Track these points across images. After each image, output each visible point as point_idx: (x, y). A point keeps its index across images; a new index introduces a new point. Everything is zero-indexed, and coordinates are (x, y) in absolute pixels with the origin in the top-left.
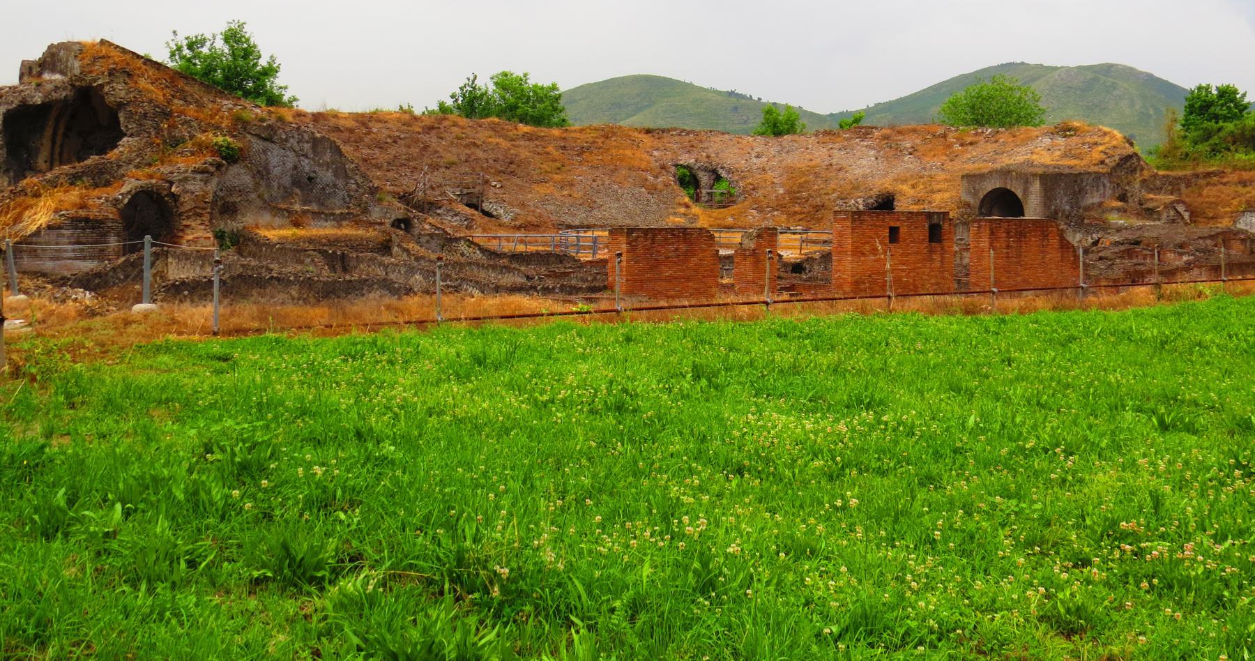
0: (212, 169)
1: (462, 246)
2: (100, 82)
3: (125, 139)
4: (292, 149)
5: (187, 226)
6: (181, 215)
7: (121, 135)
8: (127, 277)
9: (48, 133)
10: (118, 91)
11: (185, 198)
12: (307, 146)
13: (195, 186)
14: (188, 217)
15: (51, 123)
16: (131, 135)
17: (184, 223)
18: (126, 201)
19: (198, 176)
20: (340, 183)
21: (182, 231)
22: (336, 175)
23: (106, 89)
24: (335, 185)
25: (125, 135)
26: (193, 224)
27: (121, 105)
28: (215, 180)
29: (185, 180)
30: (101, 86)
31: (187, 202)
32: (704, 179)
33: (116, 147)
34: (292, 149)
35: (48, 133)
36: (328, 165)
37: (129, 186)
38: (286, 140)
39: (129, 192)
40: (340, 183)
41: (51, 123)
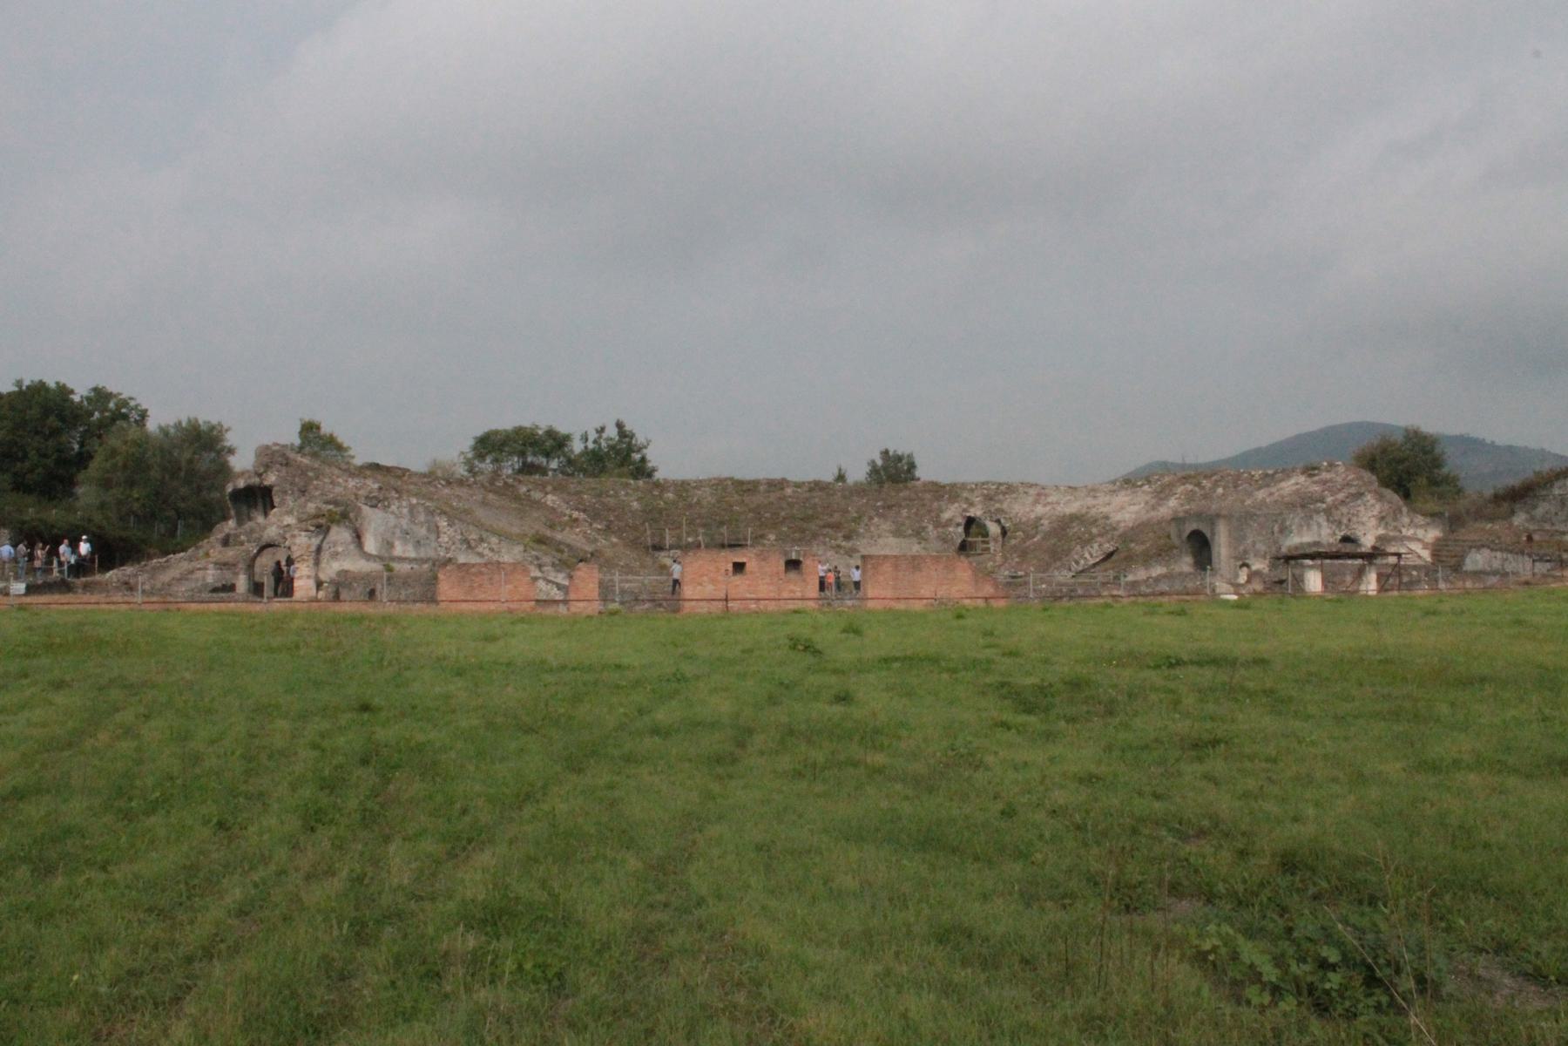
7: (273, 507)
11: (294, 548)
12: (405, 511)
22: (428, 530)
36: (422, 524)
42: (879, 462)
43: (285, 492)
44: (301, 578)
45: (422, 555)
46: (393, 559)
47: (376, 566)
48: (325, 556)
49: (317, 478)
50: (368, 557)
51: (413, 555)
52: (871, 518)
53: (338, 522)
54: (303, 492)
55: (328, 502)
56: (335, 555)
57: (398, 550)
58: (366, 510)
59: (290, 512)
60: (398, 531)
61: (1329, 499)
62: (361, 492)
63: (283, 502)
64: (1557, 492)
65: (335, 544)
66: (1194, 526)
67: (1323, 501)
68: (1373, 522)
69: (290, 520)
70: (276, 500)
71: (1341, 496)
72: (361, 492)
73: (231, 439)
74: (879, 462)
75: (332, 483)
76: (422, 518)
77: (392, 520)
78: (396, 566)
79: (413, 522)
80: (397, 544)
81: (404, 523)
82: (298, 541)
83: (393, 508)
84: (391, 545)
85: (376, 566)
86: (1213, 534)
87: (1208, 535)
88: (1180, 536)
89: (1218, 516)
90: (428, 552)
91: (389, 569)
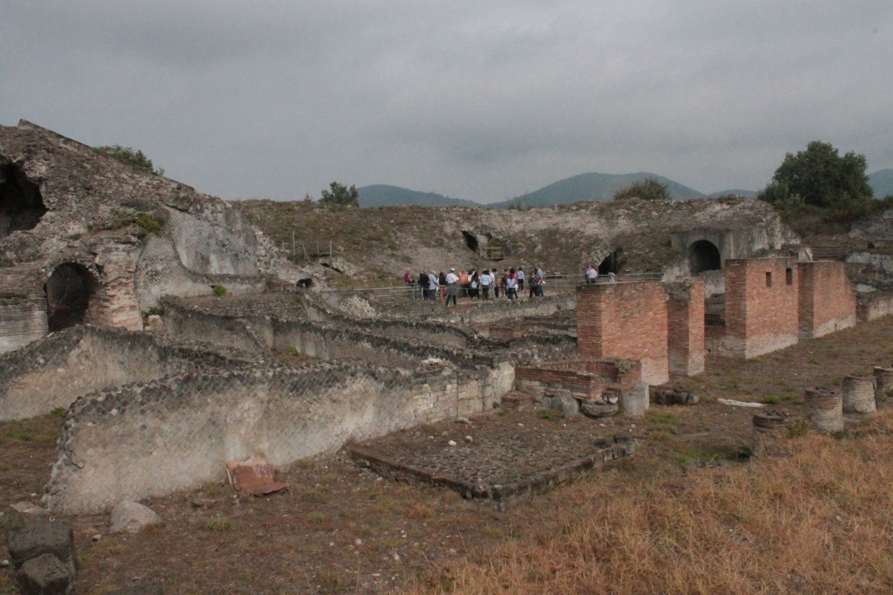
0: (134, 239)
2: (19, 158)
3: (48, 214)
4: (206, 219)
5: (113, 296)
6: (106, 285)
8: (47, 361)
10: (39, 169)
11: (109, 268)
12: (220, 216)
14: (113, 287)
16: (54, 209)
17: (111, 293)
18: (50, 274)
19: (121, 246)
21: (108, 301)
22: (247, 242)
23: (26, 165)
24: (246, 251)
25: (48, 210)
26: (118, 294)
27: (41, 180)
30: (21, 162)
31: (112, 272)
33: (39, 221)
34: (206, 219)
38: (202, 211)
39: (52, 265)
40: (250, 249)
42: (330, 192)
43: (65, 189)
44: (121, 309)
45: (241, 271)
46: (223, 277)
47: (204, 288)
48: (142, 278)
49: (98, 172)
50: (194, 276)
51: (232, 272)
52: (395, 233)
53: (157, 231)
55: (127, 205)
56: (154, 276)
57: (215, 267)
58: (176, 215)
59: (74, 218)
60: (213, 242)
61: (764, 219)
62: (162, 191)
63: (62, 204)
64: (886, 216)
65: (153, 260)
67: (761, 221)
68: (780, 235)
69: (75, 228)
70: (50, 199)
71: (769, 217)
72: (162, 191)
74: (330, 192)
75: (116, 178)
76: (239, 226)
77: (206, 228)
78: (228, 287)
79: (230, 232)
80: (213, 258)
81: (219, 231)
82: (113, 257)
83: (207, 212)
85: (204, 288)
86: (722, 242)
87: (717, 245)
88: (683, 245)
89: (728, 231)
90: (247, 268)
91: (218, 292)
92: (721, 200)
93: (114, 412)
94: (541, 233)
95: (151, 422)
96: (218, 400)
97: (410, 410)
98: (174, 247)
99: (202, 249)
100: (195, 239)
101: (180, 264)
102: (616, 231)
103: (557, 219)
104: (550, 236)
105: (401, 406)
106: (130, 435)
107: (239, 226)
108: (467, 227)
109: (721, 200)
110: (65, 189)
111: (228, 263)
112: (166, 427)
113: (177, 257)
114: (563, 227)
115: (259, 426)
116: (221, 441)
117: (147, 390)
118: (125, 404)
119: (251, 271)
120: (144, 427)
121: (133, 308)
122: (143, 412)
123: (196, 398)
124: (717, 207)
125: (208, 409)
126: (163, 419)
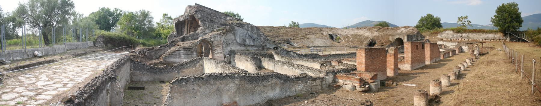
1: (291, 53)
9: (186, 27)
11: (215, 42)
13: (218, 38)
15: (186, 25)
20: (259, 38)
22: (257, 35)
28: (223, 37)
29: (215, 37)
31: (216, 43)
32: (335, 37)
35: (186, 27)
37: (200, 38)
40: (259, 38)
41: (186, 25)
43: (205, 21)
44: (218, 53)
45: (255, 44)
50: (240, 45)
51: (252, 44)
54: (212, 21)
56: (229, 44)
58: (236, 28)
60: (247, 35)
66: (398, 37)
73: (152, 15)
75: (220, 18)
76: (255, 31)
77: (245, 32)
80: (247, 40)
81: (249, 32)
84: (245, 41)
90: (258, 43)
92: (404, 27)
93: (184, 83)
94: (352, 35)
95: (196, 88)
96: (221, 83)
97: (293, 89)
98: (235, 36)
99: (244, 37)
100: (242, 35)
101: (236, 41)
102: (374, 35)
103: (357, 31)
104: (355, 36)
105: (290, 88)
106: (189, 91)
107: (255, 31)
108: (330, 33)
109: (404, 27)
110: (205, 21)
111: (252, 42)
112: (201, 90)
113: (236, 39)
114: (359, 34)
115: (235, 92)
116: (221, 96)
117: (195, 78)
118: (188, 81)
119: (259, 44)
120: (194, 89)
121: (221, 53)
122: (193, 84)
123: (212, 82)
124: (403, 29)
125: (217, 86)
126: (200, 87)
